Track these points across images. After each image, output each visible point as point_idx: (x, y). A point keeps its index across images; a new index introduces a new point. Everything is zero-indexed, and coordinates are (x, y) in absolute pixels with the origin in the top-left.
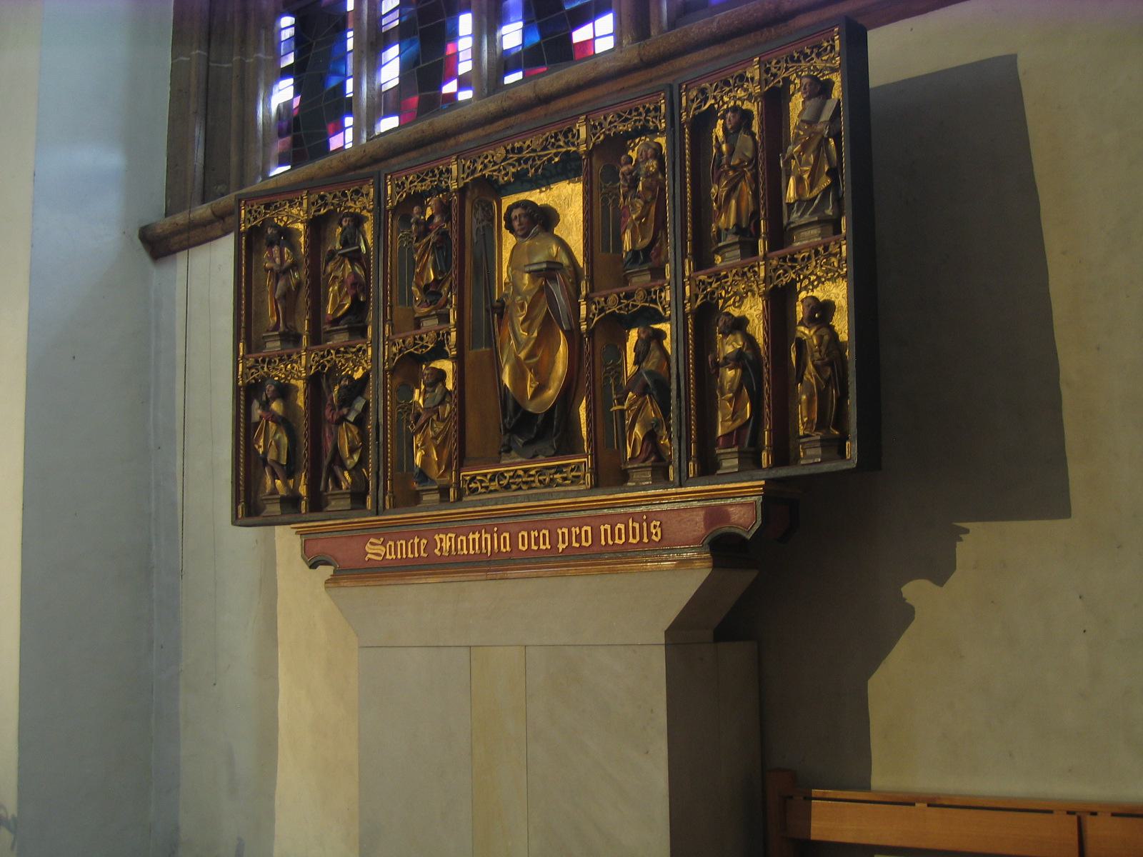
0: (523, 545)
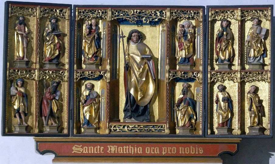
0: (148, 151)
